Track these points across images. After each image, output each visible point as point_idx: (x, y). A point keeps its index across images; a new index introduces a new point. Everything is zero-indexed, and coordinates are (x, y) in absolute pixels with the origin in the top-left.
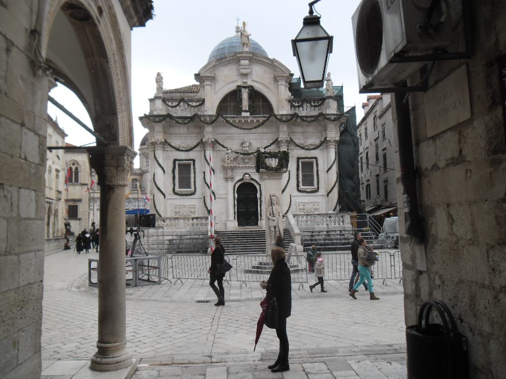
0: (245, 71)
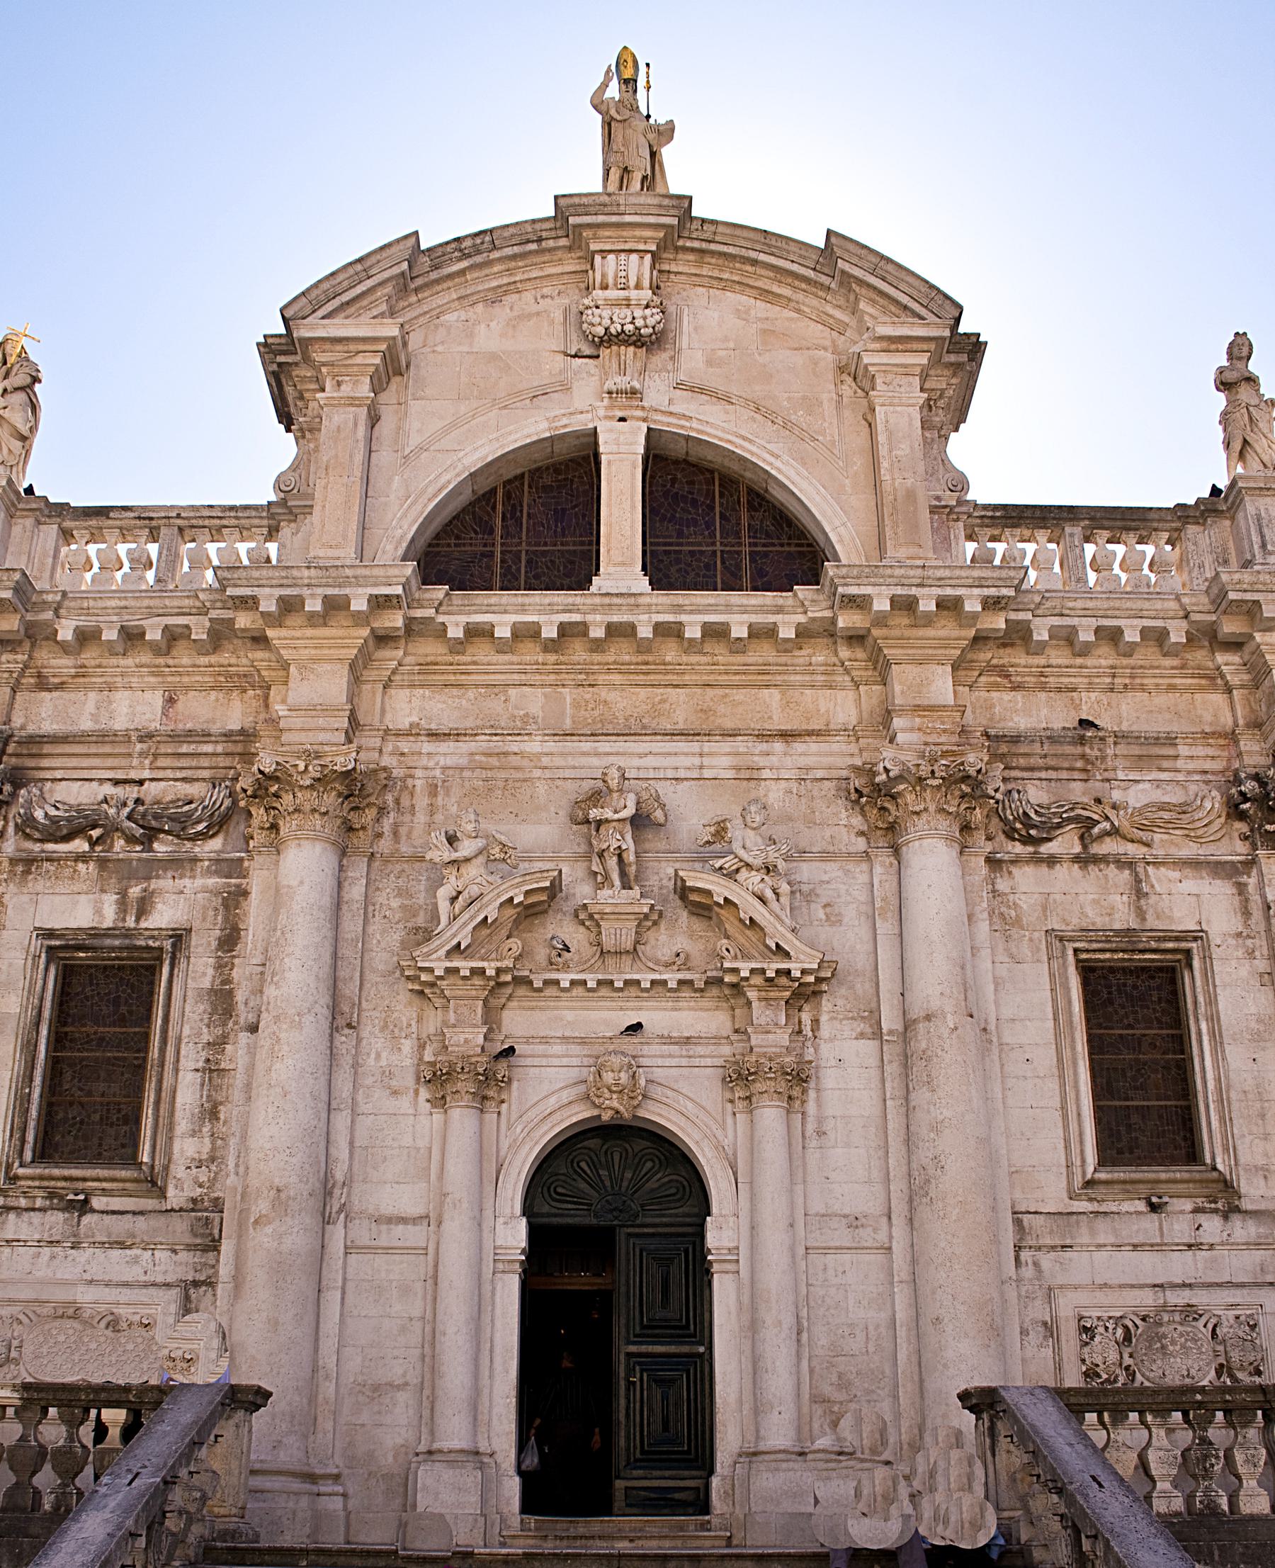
0: (620, 320)
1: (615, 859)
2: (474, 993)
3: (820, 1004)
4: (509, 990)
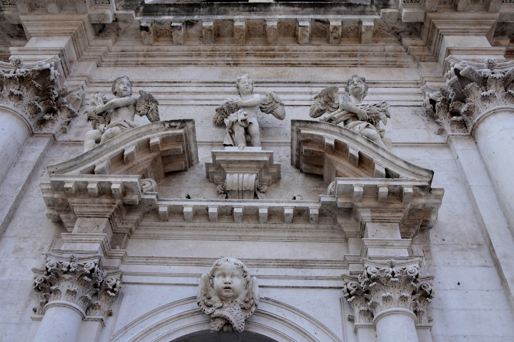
1: (242, 130)
2: (101, 210)
3: (428, 238)
4: (135, 217)
